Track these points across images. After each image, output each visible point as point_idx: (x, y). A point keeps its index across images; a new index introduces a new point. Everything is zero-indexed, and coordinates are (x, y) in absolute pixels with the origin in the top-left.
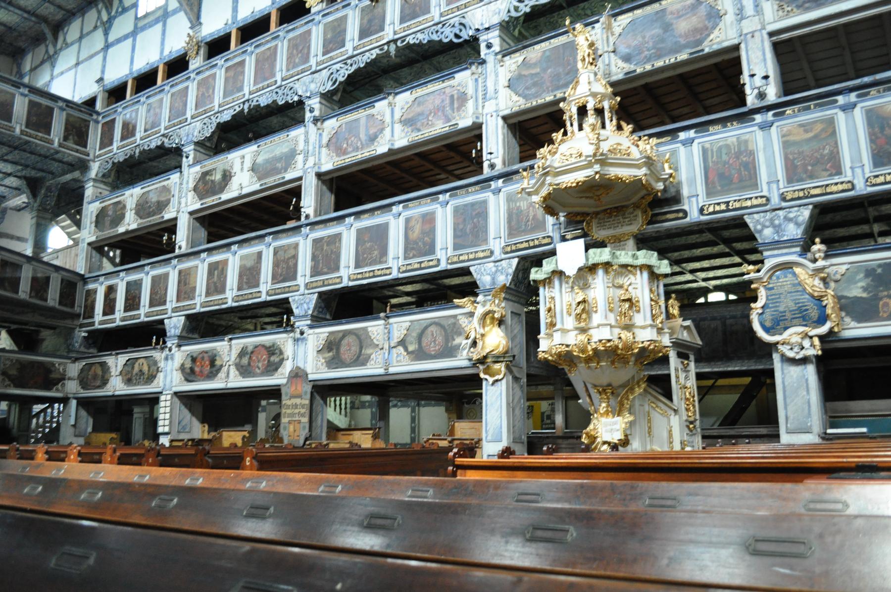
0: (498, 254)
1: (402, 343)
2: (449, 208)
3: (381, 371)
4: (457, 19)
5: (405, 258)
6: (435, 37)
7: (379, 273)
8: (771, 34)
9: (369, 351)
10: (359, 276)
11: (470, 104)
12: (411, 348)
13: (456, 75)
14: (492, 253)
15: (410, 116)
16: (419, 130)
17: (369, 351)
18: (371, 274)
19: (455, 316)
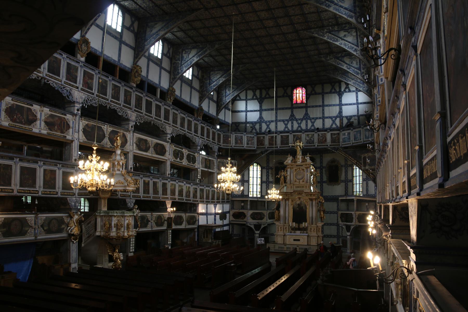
0: (77, 194)
1: (42, 226)
2: (61, 171)
3: (33, 238)
4: (69, 89)
5: (44, 188)
6: (60, 90)
7: (33, 192)
8: (134, 153)
9: (27, 229)
10: (22, 191)
11: (71, 130)
12: (45, 228)
13: (67, 115)
14: (74, 194)
15: (48, 121)
16: (51, 130)
17: (27, 229)
18: (29, 192)
19: (62, 217)
